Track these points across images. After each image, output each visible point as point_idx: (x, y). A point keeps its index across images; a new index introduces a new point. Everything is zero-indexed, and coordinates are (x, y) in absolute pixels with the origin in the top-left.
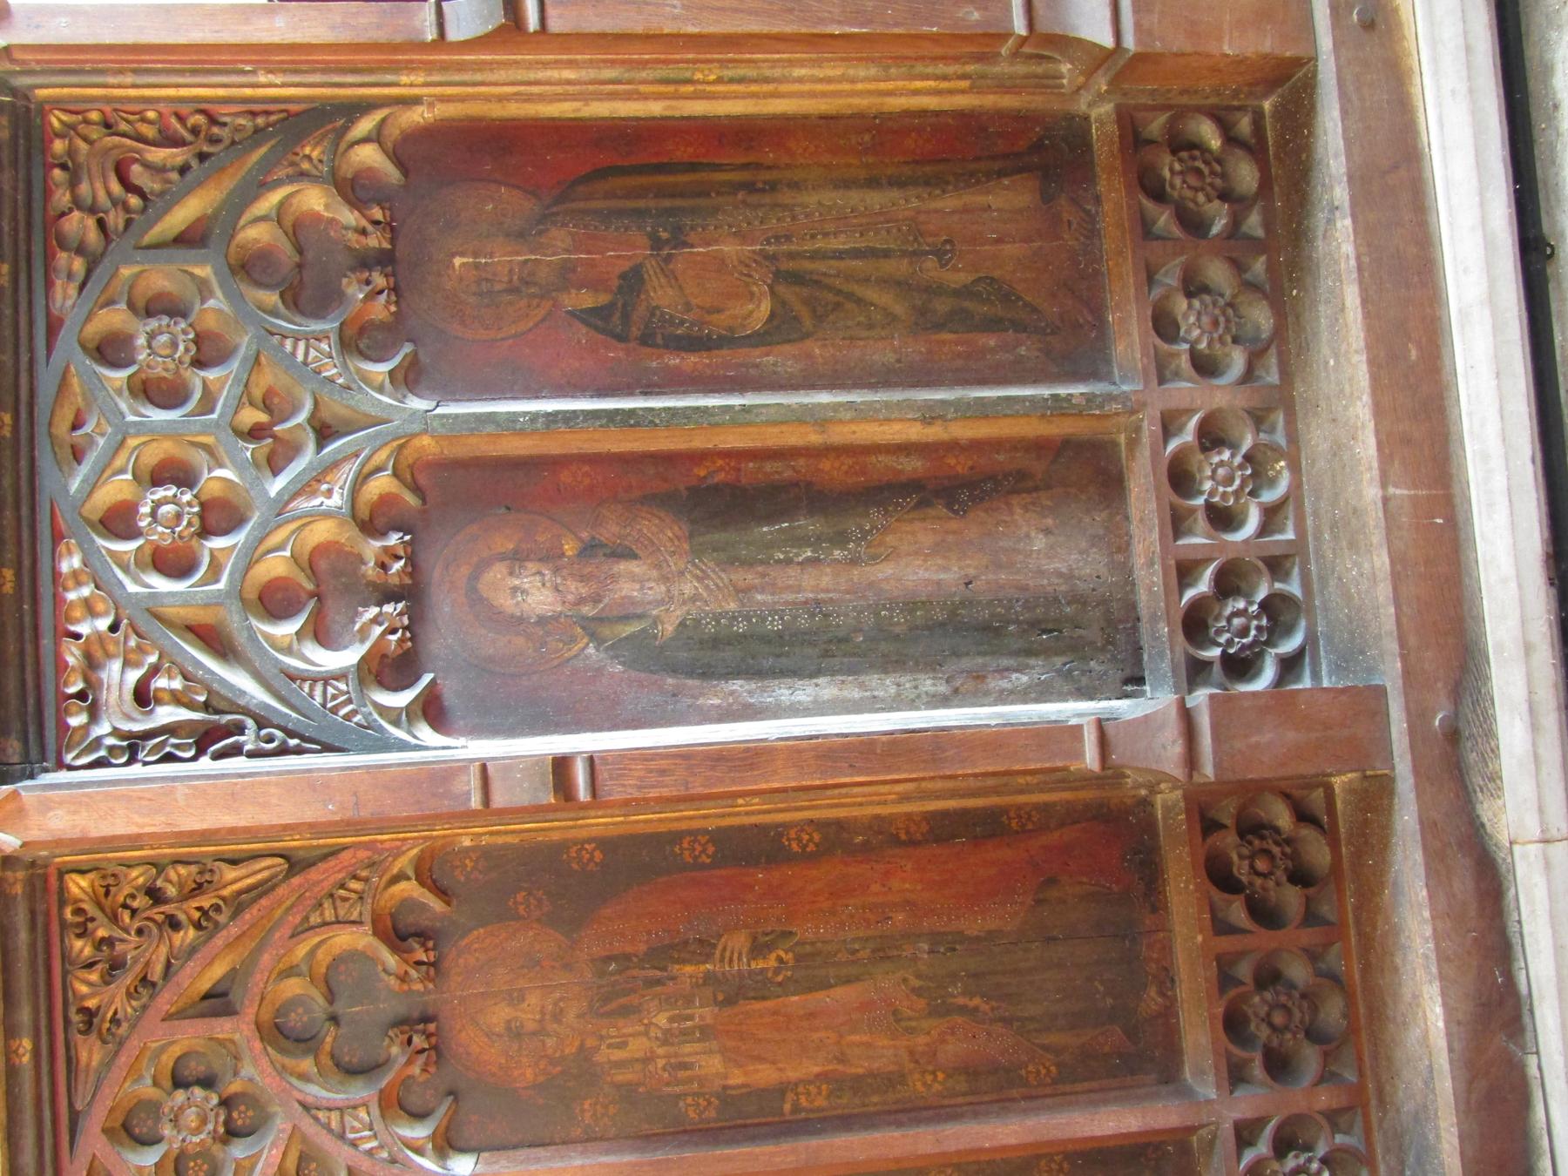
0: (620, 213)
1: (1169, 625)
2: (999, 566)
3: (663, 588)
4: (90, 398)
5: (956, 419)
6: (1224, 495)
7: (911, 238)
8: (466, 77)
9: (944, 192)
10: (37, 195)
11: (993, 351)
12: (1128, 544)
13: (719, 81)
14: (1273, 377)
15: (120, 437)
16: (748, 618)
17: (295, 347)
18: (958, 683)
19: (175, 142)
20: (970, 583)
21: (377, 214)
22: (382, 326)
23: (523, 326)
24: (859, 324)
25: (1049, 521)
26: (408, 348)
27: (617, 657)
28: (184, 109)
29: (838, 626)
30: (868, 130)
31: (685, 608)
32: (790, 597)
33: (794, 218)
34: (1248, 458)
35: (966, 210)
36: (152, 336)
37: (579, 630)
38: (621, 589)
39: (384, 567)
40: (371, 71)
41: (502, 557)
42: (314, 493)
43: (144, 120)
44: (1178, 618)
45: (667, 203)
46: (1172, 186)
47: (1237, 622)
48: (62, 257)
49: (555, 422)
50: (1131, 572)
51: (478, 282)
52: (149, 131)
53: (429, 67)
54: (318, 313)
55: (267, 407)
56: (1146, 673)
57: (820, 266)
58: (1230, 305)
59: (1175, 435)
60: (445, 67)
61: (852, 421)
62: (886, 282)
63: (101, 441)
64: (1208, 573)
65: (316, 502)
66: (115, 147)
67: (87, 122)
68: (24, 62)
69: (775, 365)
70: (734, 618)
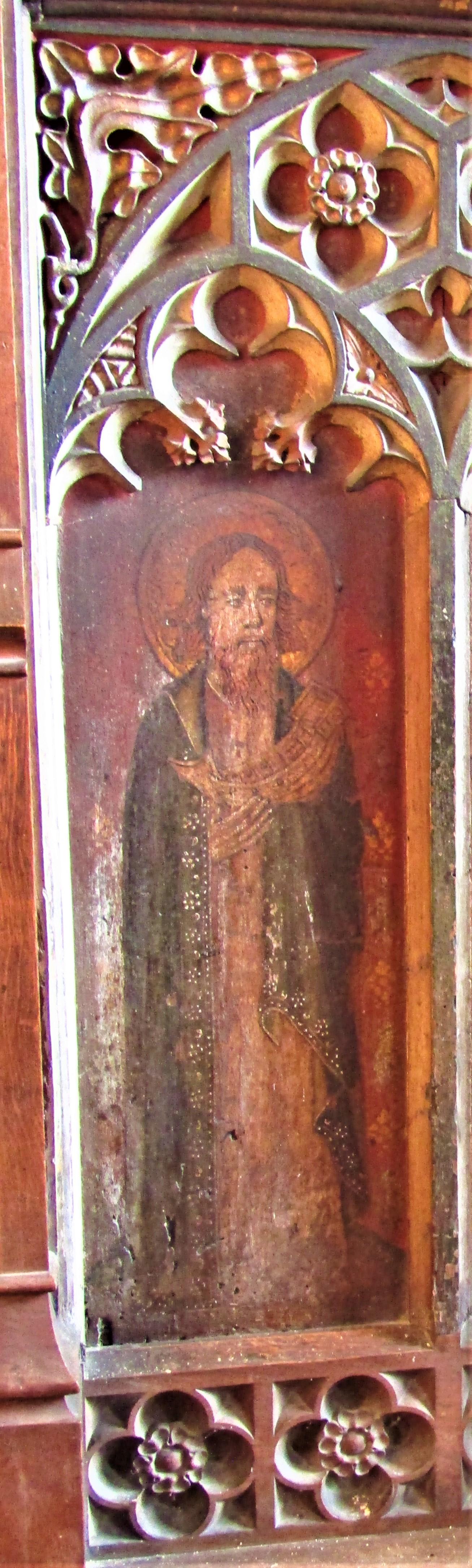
1: (174, 1374)
2: (254, 1171)
3: (238, 769)
5: (432, 1125)
6: (330, 1443)
12: (276, 1327)
15: (437, 135)
16: (199, 869)
18: (112, 1118)
20: (235, 1137)
25: (306, 1233)
27: (156, 710)
29: (186, 978)
31: (212, 794)
32: (224, 919)
34: (375, 1472)
37: (190, 667)
38: (238, 719)
39: (274, 438)
41: (282, 579)
42: (364, 360)
44: (182, 1386)
47: (177, 1456)
50: (242, 1329)
56: (116, 1347)
59: (406, 1384)
61: (433, 1002)
63: (434, 114)
64: (237, 1423)
65: (354, 362)
70: (199, 853)
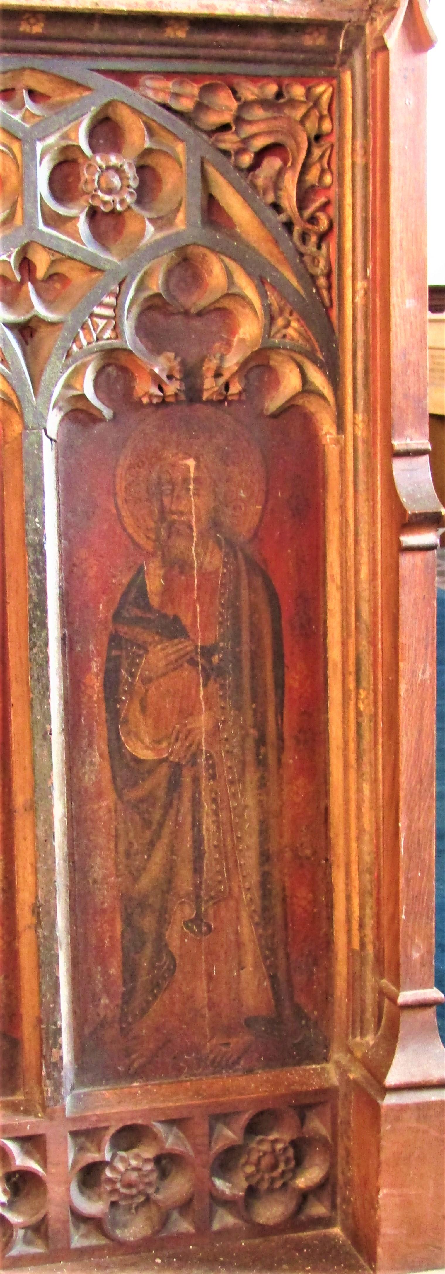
0: (237, 618)
4: (58, 108)
5: (38, 937)
7: (212, 894)
8: (362, 477)
9: (257, 925)
10: (251, 69)
11: (105, 973)
13: (359, 713)
14: (77, 1241)
15: (20, 135)
17: (107, 306)
19: (302, 201)
21: (235, 388)
22: (129, 390)
23: (128, 521)
24: (130, 843)
26: (107, 413)
28: (333, 211)
30: (314, 853)
33: (232, 782)
35: (239, 945)
36: (118, 170)
40: (366, 386)
43: (323, 172)
45: (246, 664)
46: (261, 1142)
48: (194, 89)
49: (35, 550)
51: (171, 482)
52: (313, 176)
53: (370, 442)
54: (141, 329)
55: (51, 277)
57: (186, 805)
58: (148, 1199)
59: (22, 1148)
60: (371, 456)
61: (36, 837)
62: (170, 870)
63: (17, 117)
66: (298, 144)
67: (321, 118)
68: (374, 63)
69: (92, 763)
